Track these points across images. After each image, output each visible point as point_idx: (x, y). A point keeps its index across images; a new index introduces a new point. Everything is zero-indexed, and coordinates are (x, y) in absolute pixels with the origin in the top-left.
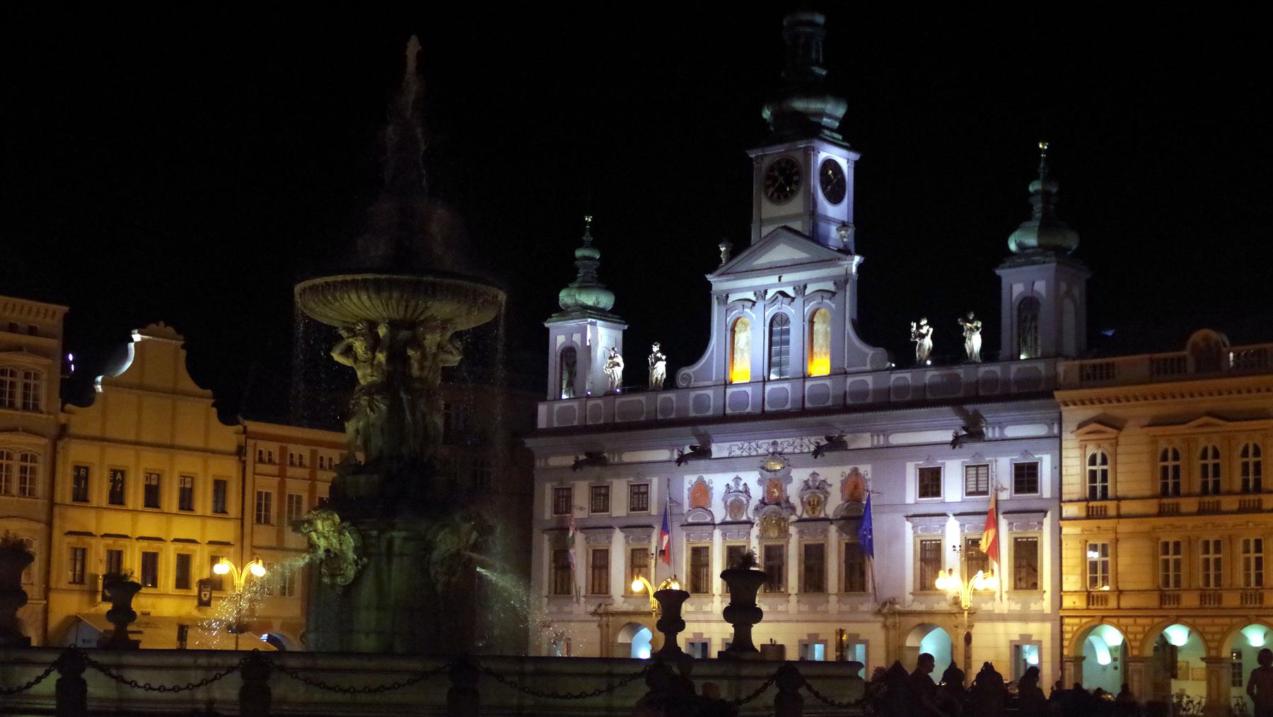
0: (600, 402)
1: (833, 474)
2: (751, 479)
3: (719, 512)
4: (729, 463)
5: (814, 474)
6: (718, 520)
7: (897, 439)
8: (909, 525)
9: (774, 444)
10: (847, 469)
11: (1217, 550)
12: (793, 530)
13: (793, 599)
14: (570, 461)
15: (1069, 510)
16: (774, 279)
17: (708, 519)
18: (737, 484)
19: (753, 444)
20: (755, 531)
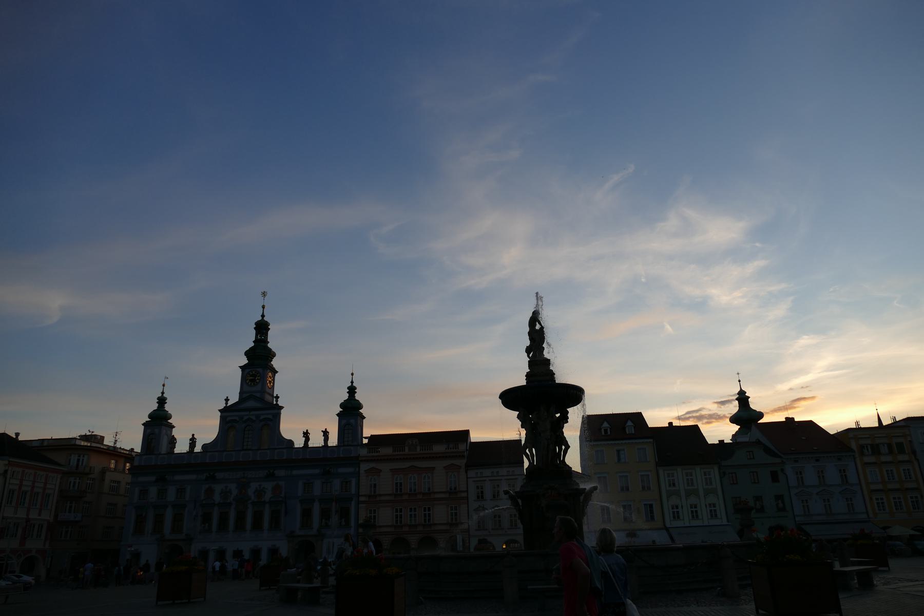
3: (217, 498)
7: (295, 472)
14: (153, 478)
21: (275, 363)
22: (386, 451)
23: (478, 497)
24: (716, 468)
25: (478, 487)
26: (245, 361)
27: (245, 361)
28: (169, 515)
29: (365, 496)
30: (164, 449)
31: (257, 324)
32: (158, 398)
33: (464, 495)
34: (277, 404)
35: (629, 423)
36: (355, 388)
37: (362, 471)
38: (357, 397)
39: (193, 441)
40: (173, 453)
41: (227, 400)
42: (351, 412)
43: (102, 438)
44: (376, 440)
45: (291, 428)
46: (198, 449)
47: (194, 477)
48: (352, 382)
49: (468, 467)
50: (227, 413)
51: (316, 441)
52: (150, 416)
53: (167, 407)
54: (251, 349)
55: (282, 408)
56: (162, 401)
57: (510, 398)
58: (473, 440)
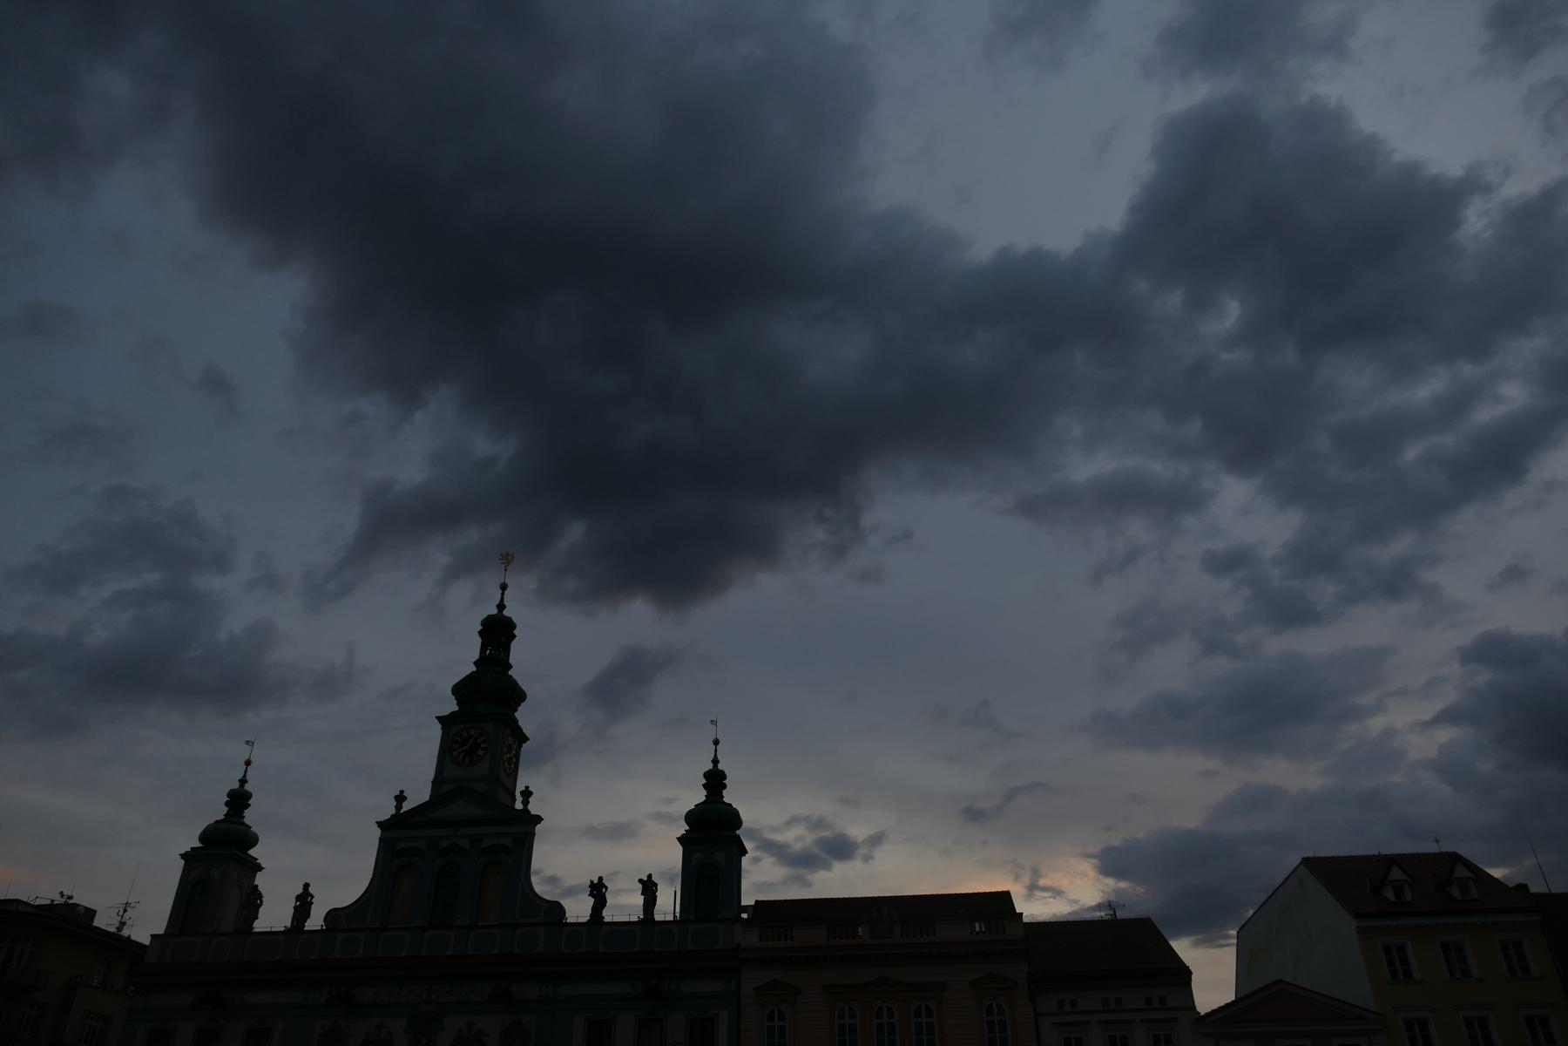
21: (526, 717)
26: (451, 706)
27: (451, 706)
32: (231, 794)
34: (526, 811)
36: (722, 775)
38: (728, 797)
39: (304, 903)
41: (400, 798)
42: (713, 834)
43: (91, 913)
46: (315, 922)
48: (715, 761)
50: (400, 832)
51: (625, 905)
52: (205, 837)
53: (250, 817)
55: (538, 819)
56: (239, 800)
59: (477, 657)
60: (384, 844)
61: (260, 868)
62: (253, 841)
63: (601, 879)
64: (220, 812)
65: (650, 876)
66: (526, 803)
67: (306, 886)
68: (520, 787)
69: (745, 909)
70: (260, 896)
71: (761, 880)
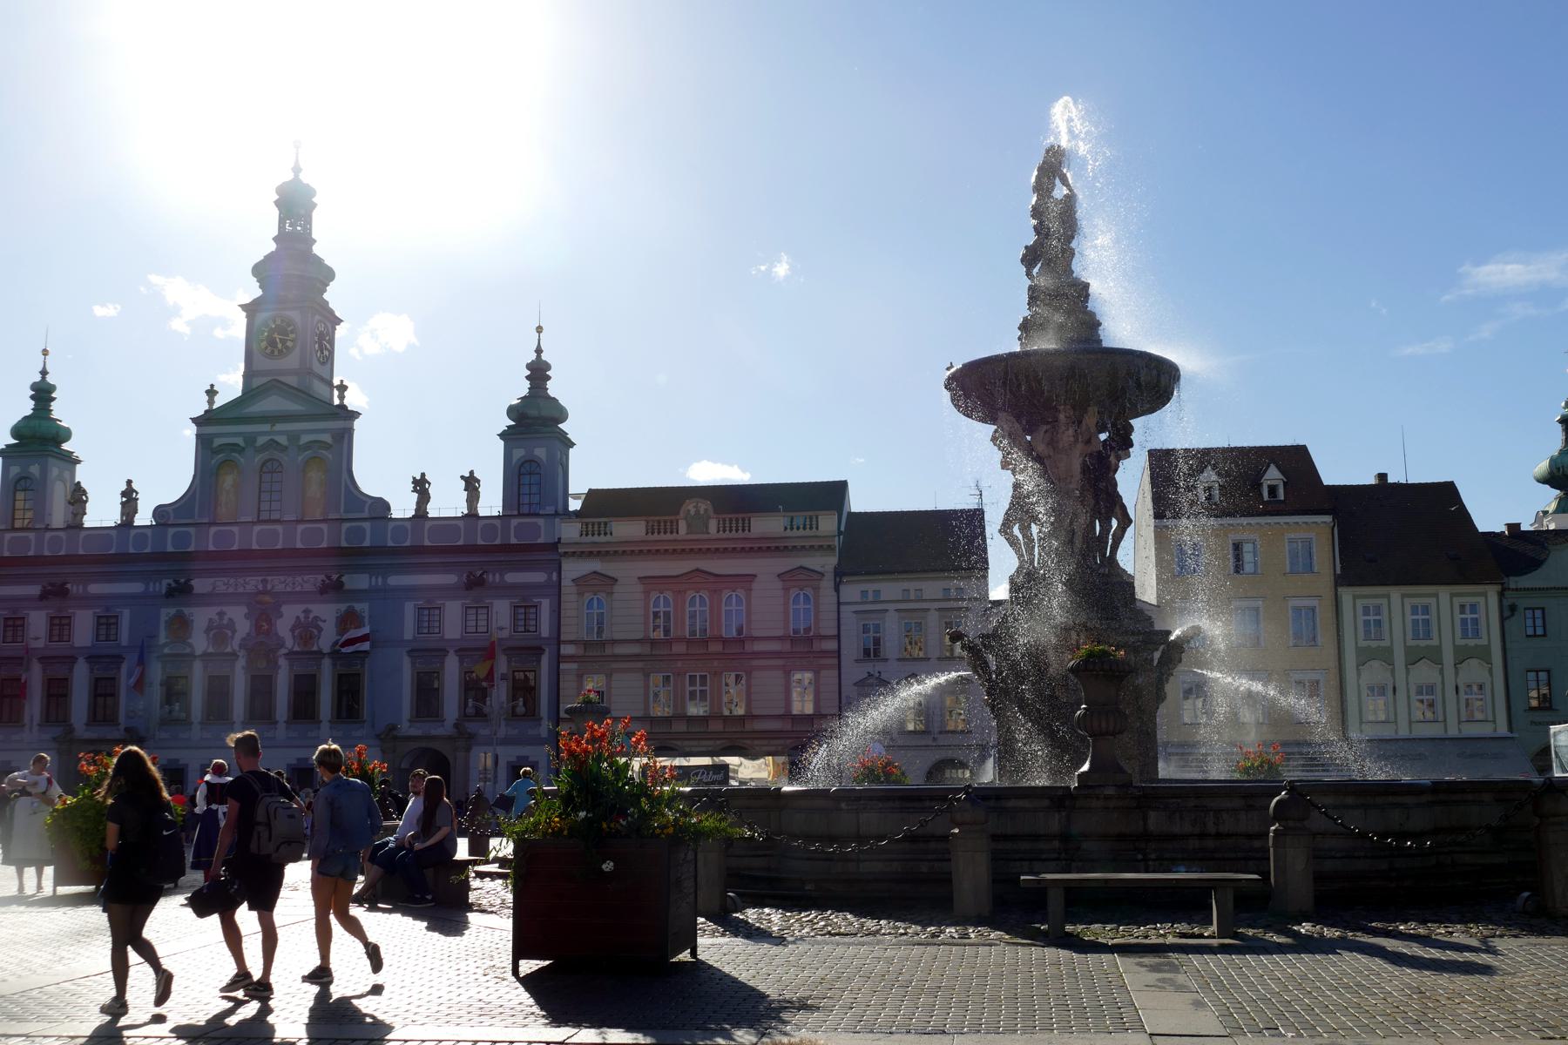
0: (61, 534)
1: (327, 612)
2: (238, 615)
4: (209, 599)
5: (307, 612)
6: (198, 652)
7: (394, 580)
8: (406, 663)
9: (265, 582)
10: (343, 607)
11: (703, 683)
12: (283, 662)
13: (281, 727)
14: (35, 590)
15: (567, 650)
16: (266, 427)
17: (188, 650)
18: (221, 619)
19: (241, 580)
20: (241, 663)
22: (628, 530)
23: (867, 652)
24: (1492, 592)
25: (866, 629)
26: (252, 291)
27: (252, 291)
28: (81, 678)
29: (571, 642)
30: (58, 515)
31: (280, 190)
32: (34, 387)
33: (831, 645)
34: (342, 407)
35: (1273, 475)
37: (566, 582)
38: (553, 389)
39: (129, 499)
40: (80, 526)
41: (211, 393)
42: (535, 428)
44: (604, 503)
45: (381, 471)
46: (144, 518)
47: (136, 587)
48: (539, 351)
49: (840, 574)
51: (447, 503)
52: (16, 431)
53: (58, 410)
54: (269, 258)
55: (354, 415)
57: (983, 388)
58: (853, 510)
59: (276, 233)
60: (203, 442)
61: (79, 462)
62: (66, 434)
63: (423, 475)
64: (28, 407)
65: (472, 473)
66: (342, 397)
67: (129, 482)
68: (336, 382)
69: (576, 496)
70: (84, 492)
71: (588, 472)
